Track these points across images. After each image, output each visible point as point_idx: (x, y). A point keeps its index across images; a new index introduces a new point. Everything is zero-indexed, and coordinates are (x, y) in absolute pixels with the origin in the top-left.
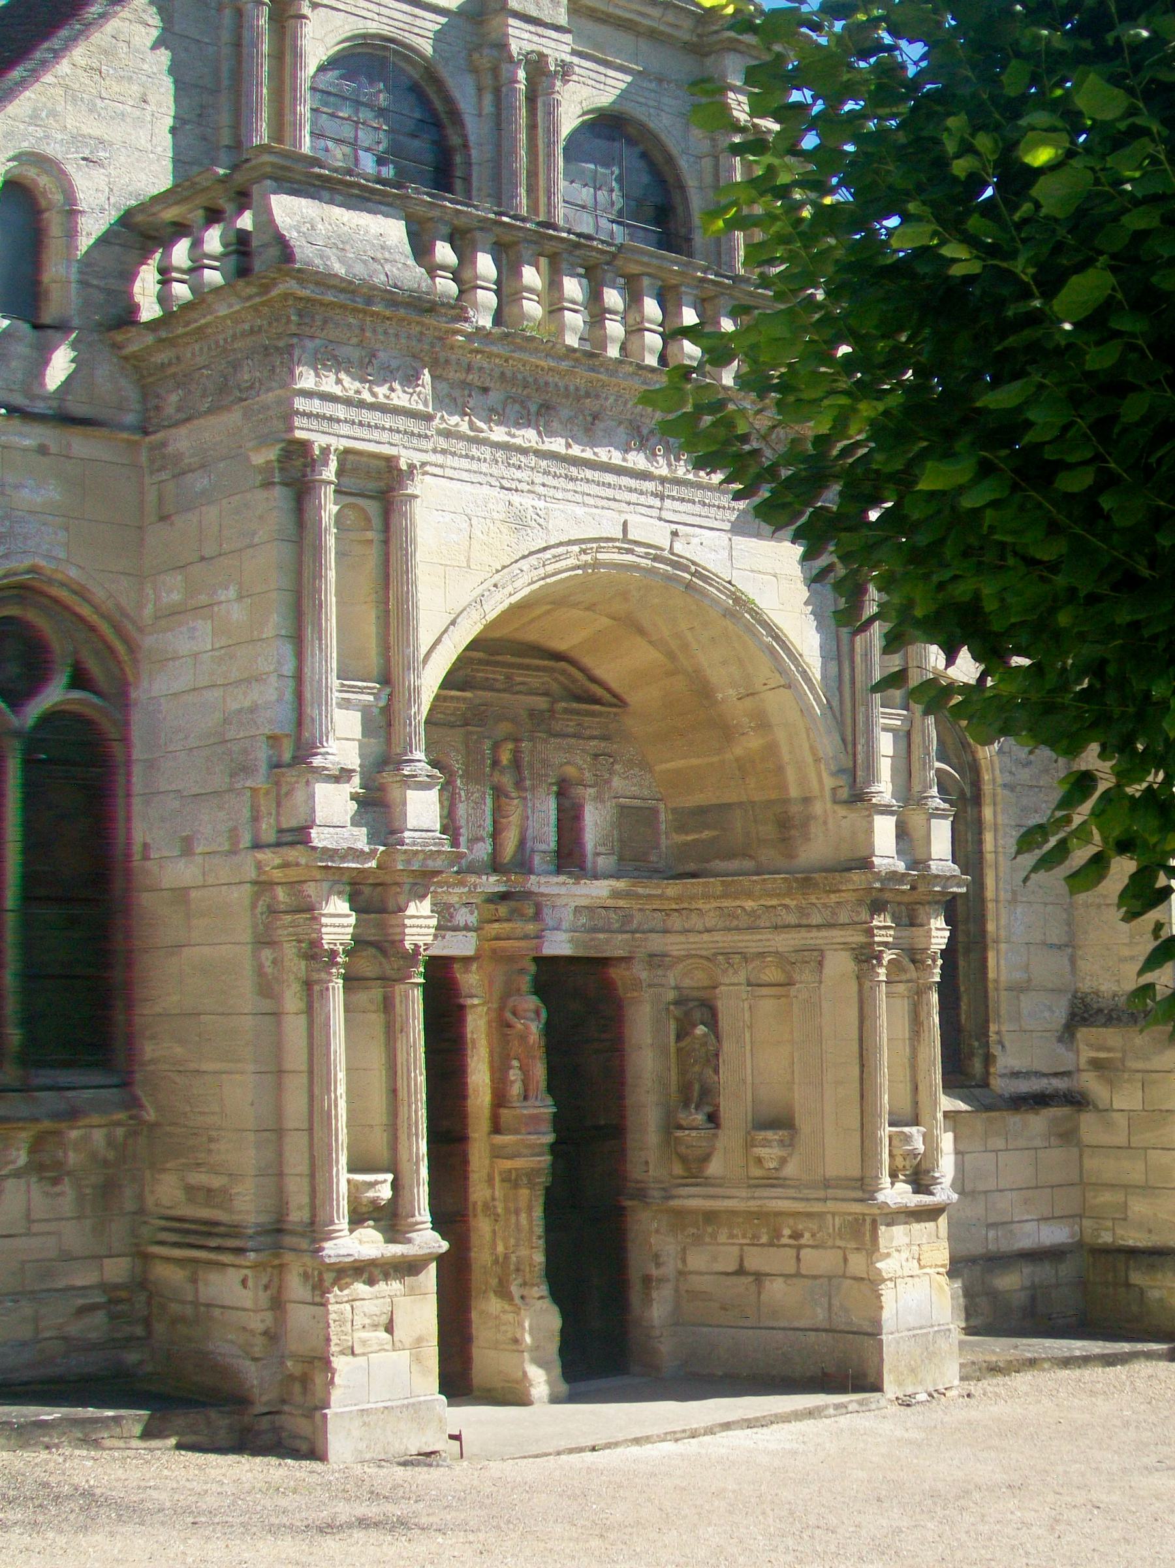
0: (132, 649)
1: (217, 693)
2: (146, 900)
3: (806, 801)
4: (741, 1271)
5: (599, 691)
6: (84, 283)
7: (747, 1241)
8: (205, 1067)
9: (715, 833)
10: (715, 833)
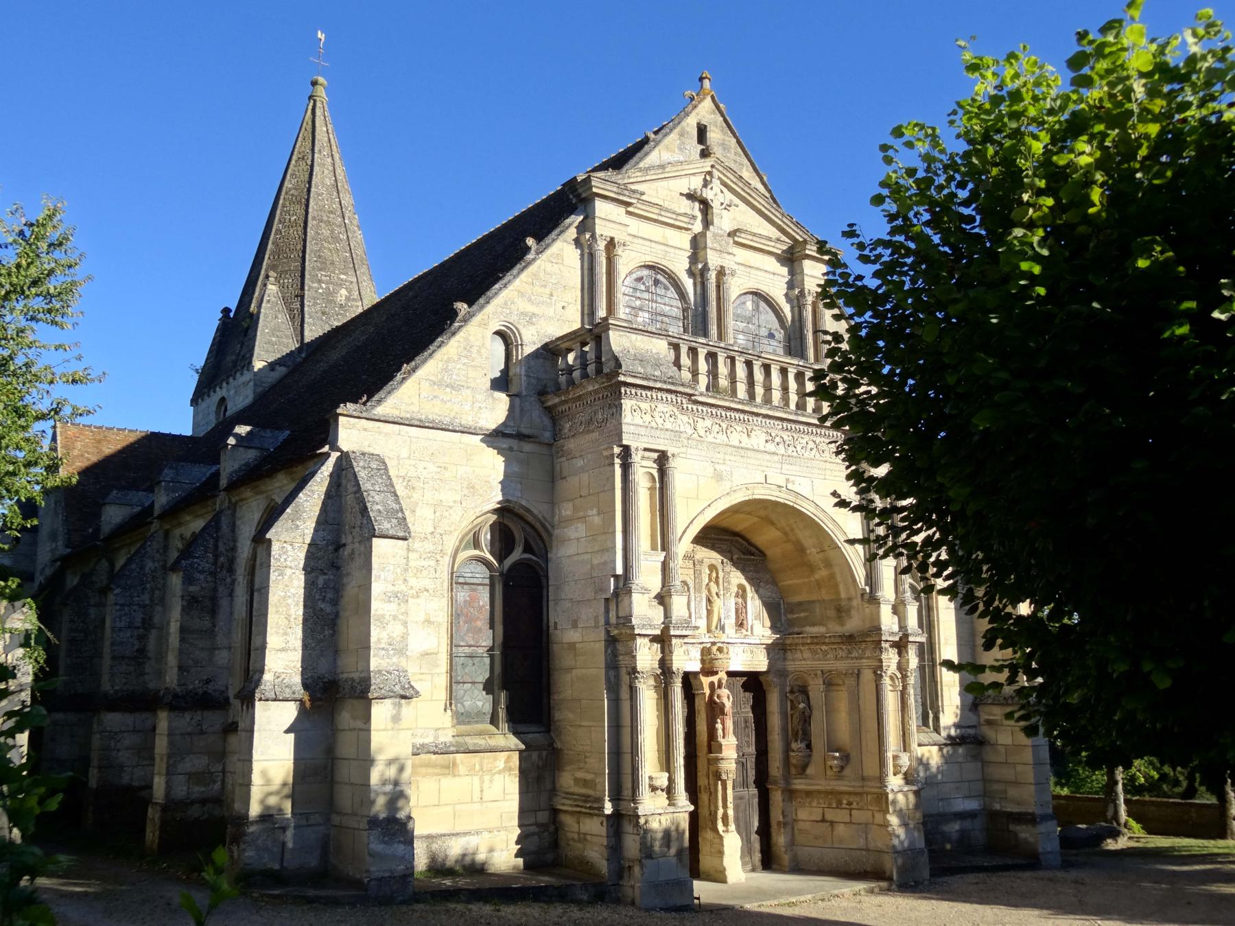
0: (550, 535)
1: (589, 556)
2: (555, 648)
3: (850, 599)
5: (753, 550)
6: (528, 376)
8: (584, 724)
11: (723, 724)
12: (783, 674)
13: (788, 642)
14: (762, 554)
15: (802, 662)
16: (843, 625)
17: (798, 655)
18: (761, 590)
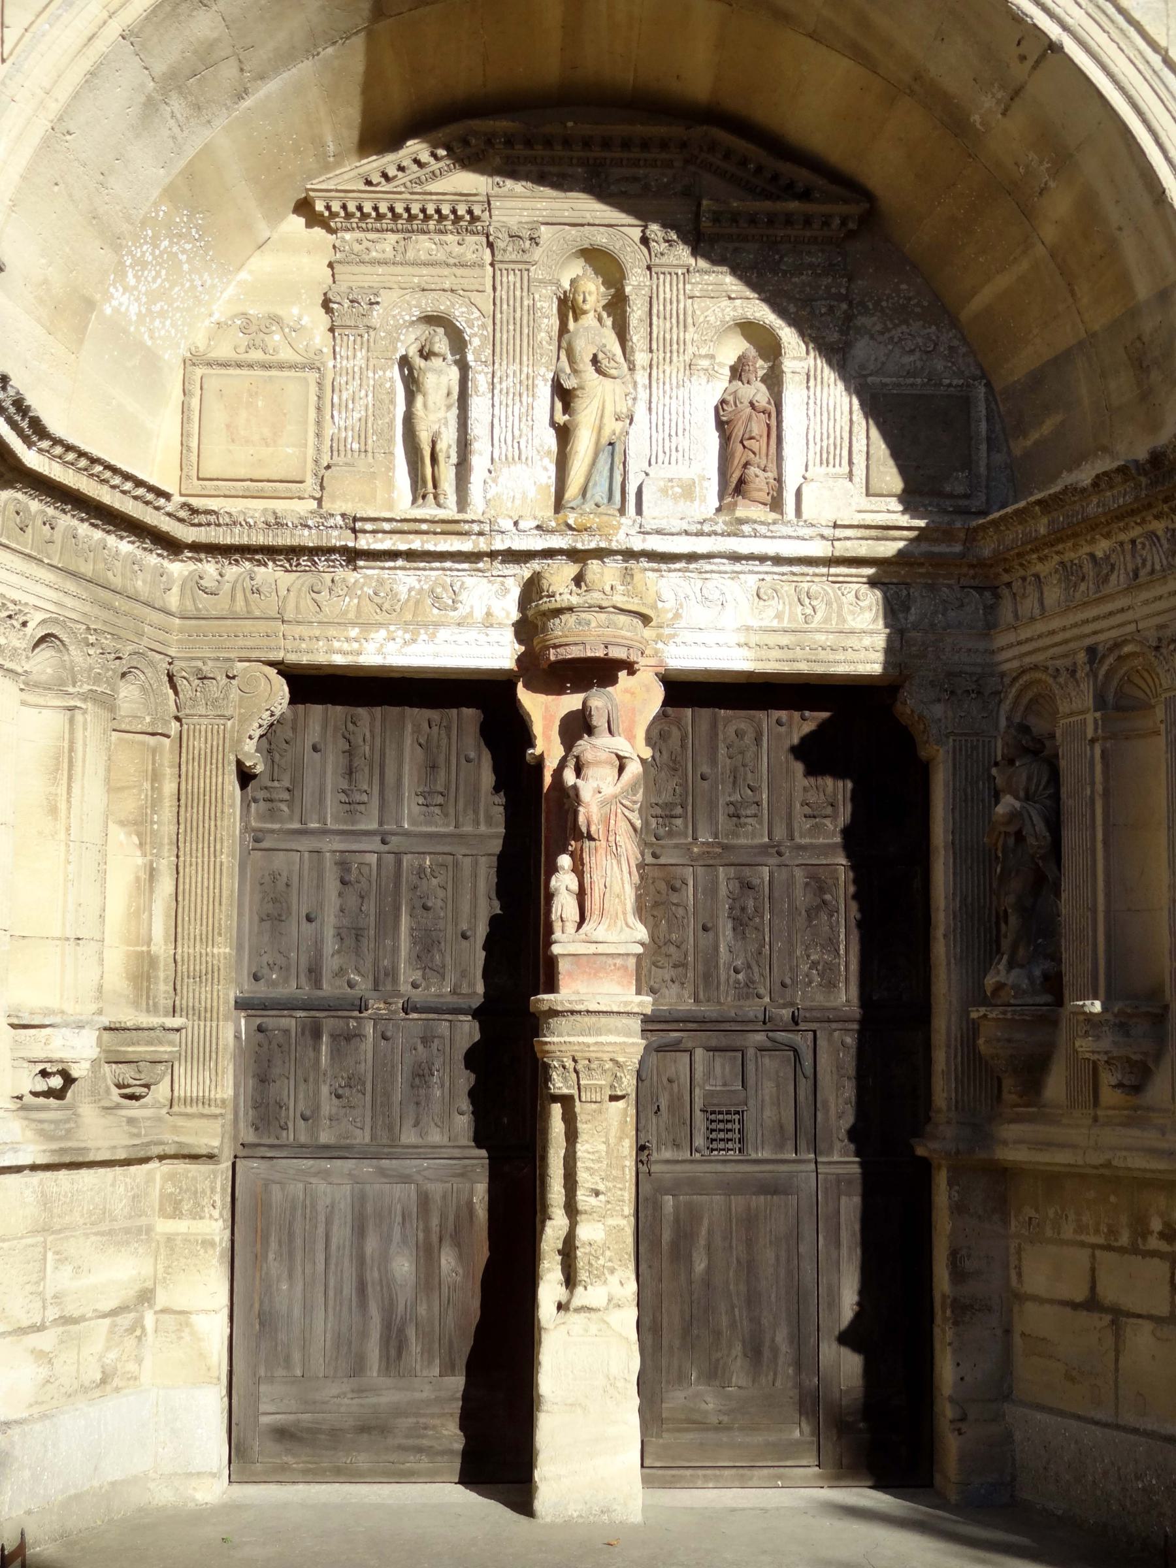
4: (1092, 1304)
5: (803, 176)
7: (1100, 1240)
9: (1058, 418)
10: (1058, 418)
11: (578, 869)
12: (977, 687)
13: (987, 548)
14: (849, 186)
15: (1046, 626)
16: (1154, 426)
17: (1029, 605)
18: (862, 349)
